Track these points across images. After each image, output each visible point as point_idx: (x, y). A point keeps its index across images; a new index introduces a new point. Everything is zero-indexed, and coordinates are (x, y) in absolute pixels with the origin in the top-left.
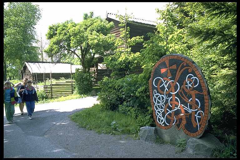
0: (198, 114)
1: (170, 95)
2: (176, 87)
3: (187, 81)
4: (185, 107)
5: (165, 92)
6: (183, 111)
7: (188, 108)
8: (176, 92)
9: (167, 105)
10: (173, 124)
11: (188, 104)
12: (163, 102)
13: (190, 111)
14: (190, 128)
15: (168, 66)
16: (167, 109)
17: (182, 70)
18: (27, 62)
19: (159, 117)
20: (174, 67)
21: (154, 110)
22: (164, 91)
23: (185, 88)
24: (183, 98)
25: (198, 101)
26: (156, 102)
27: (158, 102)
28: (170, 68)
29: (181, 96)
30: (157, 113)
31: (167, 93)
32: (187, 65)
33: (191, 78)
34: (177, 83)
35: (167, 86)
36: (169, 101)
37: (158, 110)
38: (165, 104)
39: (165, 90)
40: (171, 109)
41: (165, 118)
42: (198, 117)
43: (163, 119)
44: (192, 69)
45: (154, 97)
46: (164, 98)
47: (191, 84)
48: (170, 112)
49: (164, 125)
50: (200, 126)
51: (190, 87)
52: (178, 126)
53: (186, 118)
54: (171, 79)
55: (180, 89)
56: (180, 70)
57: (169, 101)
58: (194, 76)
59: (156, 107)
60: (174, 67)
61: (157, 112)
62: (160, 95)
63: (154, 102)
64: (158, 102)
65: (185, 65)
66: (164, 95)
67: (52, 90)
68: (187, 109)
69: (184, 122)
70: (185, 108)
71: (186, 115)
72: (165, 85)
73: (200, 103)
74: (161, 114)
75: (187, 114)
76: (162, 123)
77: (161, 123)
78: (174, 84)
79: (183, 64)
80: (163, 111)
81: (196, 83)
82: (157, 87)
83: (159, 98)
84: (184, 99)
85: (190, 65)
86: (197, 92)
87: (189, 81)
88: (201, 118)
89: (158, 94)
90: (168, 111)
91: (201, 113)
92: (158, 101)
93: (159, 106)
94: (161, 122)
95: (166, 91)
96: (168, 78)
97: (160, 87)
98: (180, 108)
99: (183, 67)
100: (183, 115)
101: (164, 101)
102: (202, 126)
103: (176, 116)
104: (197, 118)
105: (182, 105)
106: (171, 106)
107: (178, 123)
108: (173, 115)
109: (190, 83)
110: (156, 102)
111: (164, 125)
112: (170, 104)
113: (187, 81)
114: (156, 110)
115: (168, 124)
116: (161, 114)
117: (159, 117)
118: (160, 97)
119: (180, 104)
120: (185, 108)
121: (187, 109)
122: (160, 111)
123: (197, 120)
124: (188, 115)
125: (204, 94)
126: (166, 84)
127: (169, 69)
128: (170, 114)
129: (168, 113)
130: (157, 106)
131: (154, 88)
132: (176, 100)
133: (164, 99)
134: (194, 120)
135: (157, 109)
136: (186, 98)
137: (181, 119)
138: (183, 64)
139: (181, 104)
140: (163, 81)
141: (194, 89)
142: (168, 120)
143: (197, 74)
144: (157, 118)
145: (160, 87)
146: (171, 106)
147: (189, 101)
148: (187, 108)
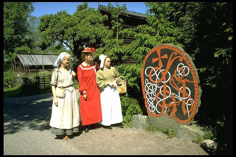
1: (161, 84)
2: (167, 77)
3: (178, 69)
4: (176, 95)
6: (174, 100)
8: (167, 82)
9: (158, 93)
10: (164, 112)
11: (179, 93)
12: (154, 91)
13: (181, 99)
14: (181, 115)
15: (159, 56)
16: (159, 98)
18: (19, 54)
19: (151, 106)
20: (166, 56)
21: (146, 99)
23: (176, 77)
25: (188, 89)
28: (162, 57)
29: (172, 84)
30: (149, 102)
32: (178, 55)
33: (182, 68)
34: (168, 72)
38: (157, 92)
39: (157, 79)
40: (162, 97)
44: (183, 59)
45: (146, 86)
47: (181, 73)
48: (161, 100)
49: (155, 113)
50: (190, 113)
51: (180, 76)
53: (177, 106)
54: (162, 68)
56: (171, 60)
60: (166, 56)
61: (149, 101)
62: (151, 84)
63: (146, 91)
64: (150, 91)
67: (44, 82)
68: (178, 98)
69: (175, 110)
70: (176, 96)
71: (176, 103)
72: (156, 74)
75: (178, 102)
76: (154, 111)
77: (153, 112)
78: (166, 73)
80: (154, 100)
81: (186, 71)
82: (148, 76)
83: (151, 87)
87: (180, 70)
88: (191, 106)
89: (150, 83)
90: (159, 100)
93: (150, 95)
95: (158, 80)
96: (159, 67)
98: (171, 97)
99: (174, 56)
100: (174, 103)
104: (187, 106)
105: (173, 94)
107: (169, 111)
108: (164, 103)
109: (180, 72)
111: (155, 113)
113: (178, 69)
114: (147, 98)
115: (159, 112)
117: (151, 106)
120: (176, 96)
121: (178, 98)
122: (151, 99)
126: (157, 73)
127: (161, 59)
128: (161, 103)
131: (145, 77)
132: (168, 89)
134: (184, 108)
135: (148, 98)
137: (171, 108)
140: (155, 71)
141: (185, 78)
142: (159, 109)
147: (180, 89)
148: (178, 96)
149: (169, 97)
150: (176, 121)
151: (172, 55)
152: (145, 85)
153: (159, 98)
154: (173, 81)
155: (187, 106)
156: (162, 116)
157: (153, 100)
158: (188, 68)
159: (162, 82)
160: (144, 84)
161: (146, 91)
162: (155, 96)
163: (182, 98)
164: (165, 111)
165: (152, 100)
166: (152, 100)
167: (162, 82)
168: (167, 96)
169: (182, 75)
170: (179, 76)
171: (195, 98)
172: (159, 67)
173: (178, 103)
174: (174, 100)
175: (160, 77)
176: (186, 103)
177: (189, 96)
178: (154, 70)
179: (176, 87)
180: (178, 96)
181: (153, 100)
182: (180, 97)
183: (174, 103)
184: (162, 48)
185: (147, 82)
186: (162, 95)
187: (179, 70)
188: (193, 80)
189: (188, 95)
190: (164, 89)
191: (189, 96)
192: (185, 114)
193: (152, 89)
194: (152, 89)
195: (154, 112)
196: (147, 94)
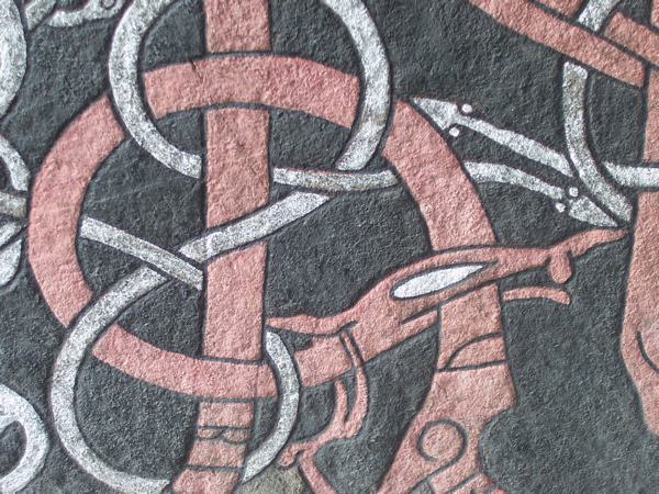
4: (502, 137)
6: (455, 216)
7: (558, 142)
9: (90, 138)
16: (95, 230)
36: (125, 49)
41: (60, 401)
57: (125, 49)
70: (507, 157)
71: (502, 284)
75: (538, 257)
103: (300, 324)
105: (447, 113)
106: (162, 151)
107: (345, 426)
112: (144, 132)
119: (377, 98)
120: (507, 157)
124: (560, 272)
129: (117, 299)
148: (561, 165)
149: (347, 183)
153: (95, 230)
162: (16, 204)
163: (625, 175)
164: (278, 439)
168: (292, 177)
173: (540, 276)
174: (455, 216)
180: (550, 157)
182: (587, 170)
183: (462, 272)
186: (188, 164)
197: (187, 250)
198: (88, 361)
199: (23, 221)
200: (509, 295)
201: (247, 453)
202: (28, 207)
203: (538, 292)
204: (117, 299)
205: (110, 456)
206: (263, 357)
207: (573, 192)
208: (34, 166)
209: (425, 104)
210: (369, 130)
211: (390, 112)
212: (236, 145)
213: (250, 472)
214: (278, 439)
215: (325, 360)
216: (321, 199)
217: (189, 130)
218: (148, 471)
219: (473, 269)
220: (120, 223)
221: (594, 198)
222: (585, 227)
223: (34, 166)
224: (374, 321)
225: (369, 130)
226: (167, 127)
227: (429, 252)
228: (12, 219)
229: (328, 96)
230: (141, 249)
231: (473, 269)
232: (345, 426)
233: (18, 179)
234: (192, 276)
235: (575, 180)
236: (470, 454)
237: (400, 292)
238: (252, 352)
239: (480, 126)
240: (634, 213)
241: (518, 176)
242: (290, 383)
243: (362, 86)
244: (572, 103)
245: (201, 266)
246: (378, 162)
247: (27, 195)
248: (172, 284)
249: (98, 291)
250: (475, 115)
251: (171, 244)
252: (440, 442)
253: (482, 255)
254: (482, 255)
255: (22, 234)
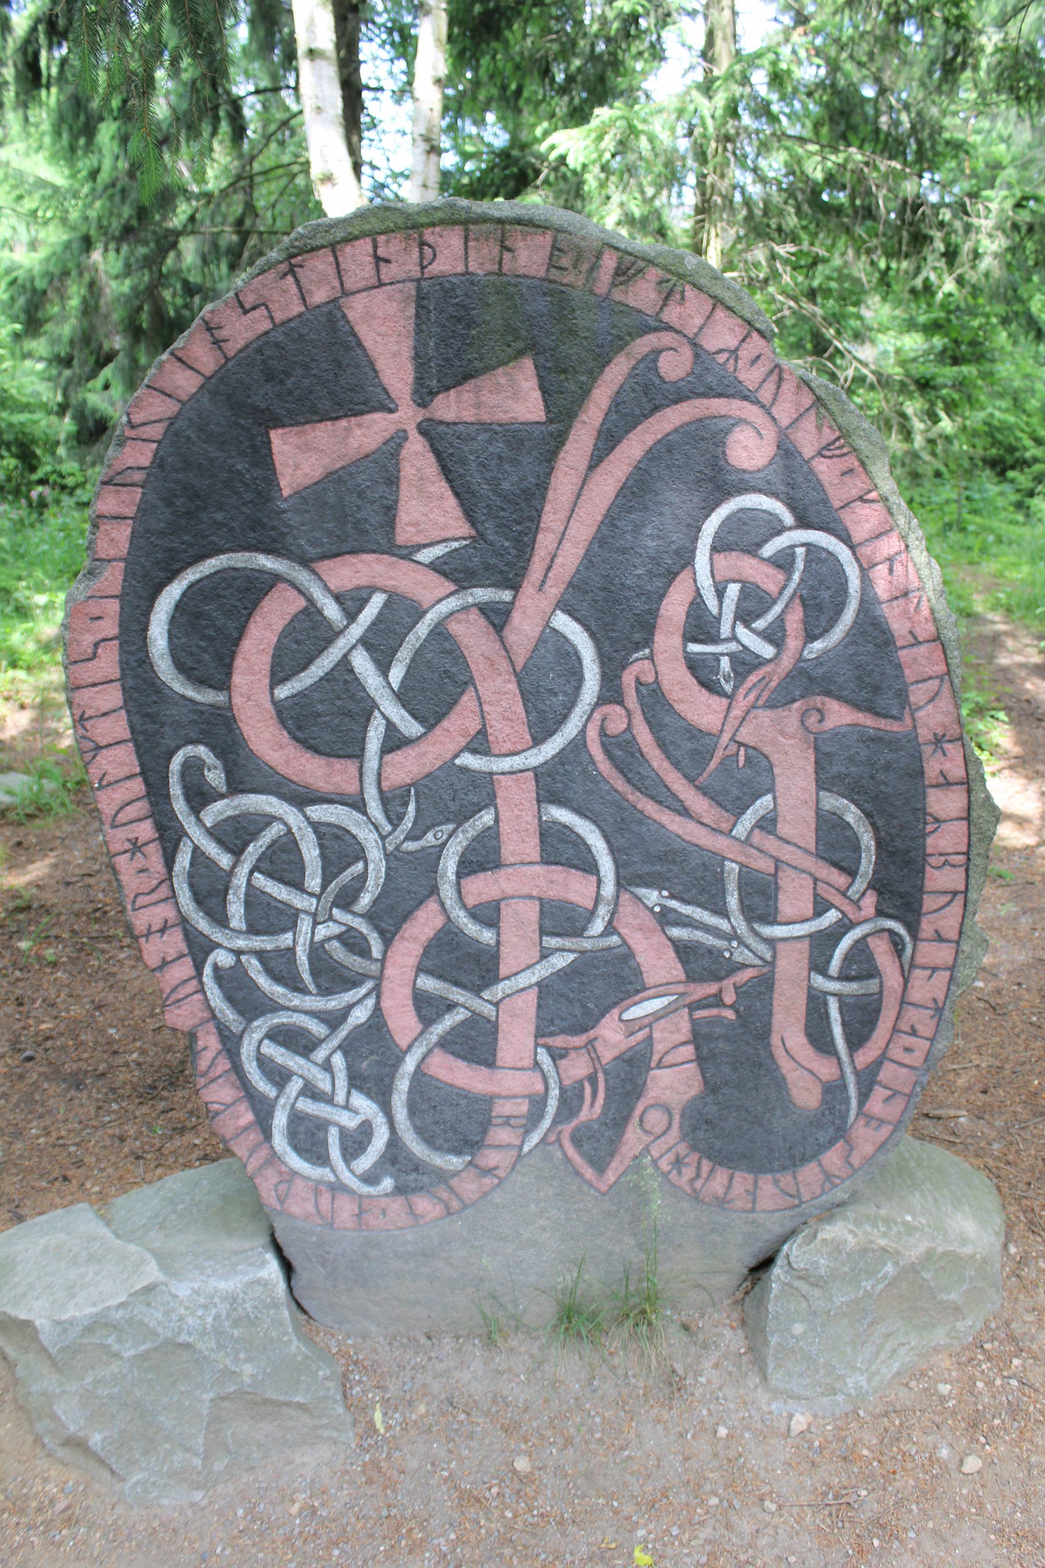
0: (847, 958)
3: (705, 582)
4: (686, 910)
5: (372, 761)
6: (657, 962)
8: (551, 748)
9: (425, 924)
10: (535, 1138)
12: (346, 900)
16: (428, 983)
17: (633, 448)
22: (359, 755)
24: (650, 808)
25: (852, 815)
26: (221, 920)
27: (267, 917)
29: (620, 784)
30: (263, 1062)
31: (405, 767)
33: (769, 550)
34: (563, 622)
35: (397, 674)
36: (449, 865)
37: (281, 1019)
42: (852, 988)
43: (365, 1106)
45: (183, 860)
46: (367, 837)
47: (760, 624)
51: (745, 663)
52: (599, 1144)
54: (457, 572)
55: (611, 692)
56: (608, 440)
57: (449, 865)
58: (803, 522)
59: (233, 983)
61: (270, 1049)
63: (203, 924)
64: (267, 917)
65: (674, 366)
66: (359, 805)
69: (674, 1083)
71: (693, 1007)
72: (362, 663)
73: (867, 839)
74: (327, 1066)
75: (712, 988)
76: (365, 1162)
79: (657, 352)
80: (360, 1015)
84: (650, 808)
85: (750, 377)
86: (840, 715)
87: (733, 590)
91: (880, 949)
92: (254, 899)
93: (281, 967)
94: (335, 1152)
95: (394, 741)
97: (283, 692)
99: (647, 395)
100: (657, 1004)
101: (363, 877)
102: (887, 1073)
103: (559, 1041)
104: (833, 1006)
105: (652, 896)
106: (472, 928)
107: (591, 1111)
108: (517, 1039)
109: (745, 616)
110: (236, 909)
113: (705, 582)
115: (455, 1162)
116: (327, 1066)
118: (288, 845)
119: (609, 889)
123: (837, 1030)
124: (729, 998)
125: (924, 734)
126: (381, 645)
127: (423, 430)
129: (439, 1029)
130: (253, 966)
133: (360, 854)
136: (698, 803)
138: (657, 352)
139: (621, 884)
140: (332, 611)
143: (836, 497)
144: (280, 1120)
145: (283, 692)
146: (472, 928)
147: (741, 830)
148: (724, 925)
149: (587, 945)
150: (696, 1196)
151: (617, 372)
152: (170, 837)
154: (644, 736)
155: (833, 1006)
156: (497, 1198)
157: (343, 1032)
158: (843, 553)
159: (468, 760)
160: (146, 830)
161: (203, 924)
162: (374, 968)
163: (768, 931)
164: (547, 1123)
165: (317, 1029)
166: (317, 1029)
167: (468, 760)
168: (553, 942)
169: (767, 651)
170: (725, 663)
171: (929, 903)
172: (407, 553)
173: (717, 1000)
174: (657, 962)
175: (436, 688)
176: (818, 981)
177: (854, 891)
178: (311, 611)
179: (684, 812)
181: (343, 1032)
182: (742, 928)
184: (435, 268)
185: (199, 797)
186: (487, 936)
187: (720, 594)
188: (902, 695)
189: (840, 880)
190: (509, 850)
191: (854, 891)
192: (806, 1095)
193: (313, 883)
194: (313, 883)
195: (370, 1178)
196: (223, 958)
197: (486, 995)
198: (419, 1073)
199: (379, 978)
200: (700, 1014)
201: (527, 1132)
202: (383, 968)
203: (714, 1012)
204: (439, 1029)
205: (430, 1141)
206: (537, 1065)
207: (735, 944)
208: (387, 941)
209: (642, 891)
210: (603, 911)
211: (617, 897)
212: (520, 922)
213: (526, 1149)
214: (547, 1123)
215: (577, 1068)
216: (572, 957)
217: (488, 915)
218: (458, 1152)
219: (672, 998)
220: (441, 977)
221: (747, 947)
222: (745, 966)
223: (387, 941)
224: (611, 1036)
225: (603, 911)
226: (474, 915)
227: (645, 989)
228: (364, 977)
229: (576, 889)
230: (457, 995)
231: (672, 998)
232: (591, 1111)
233: (376, 952)
234: (488, 1010)
235: (735, 936)
236: (675, 1132)
237: (625, 1017)
238: (528, 1062)
239: (674, 904)
240: (774, 956)
241: (699, 935)
242: (553, 1084)
243: (599, 882)
244: (732, 886)
245: (496, 1005)
246: (610, 929)
247: (383, 961)
248: (476, 1020)
249: (427, 1022)
250: (672, 896)
251: (477, 990)
252: (656, 1119)
253: (681, 988)
254: (681, 988)
255: (377, 990)
